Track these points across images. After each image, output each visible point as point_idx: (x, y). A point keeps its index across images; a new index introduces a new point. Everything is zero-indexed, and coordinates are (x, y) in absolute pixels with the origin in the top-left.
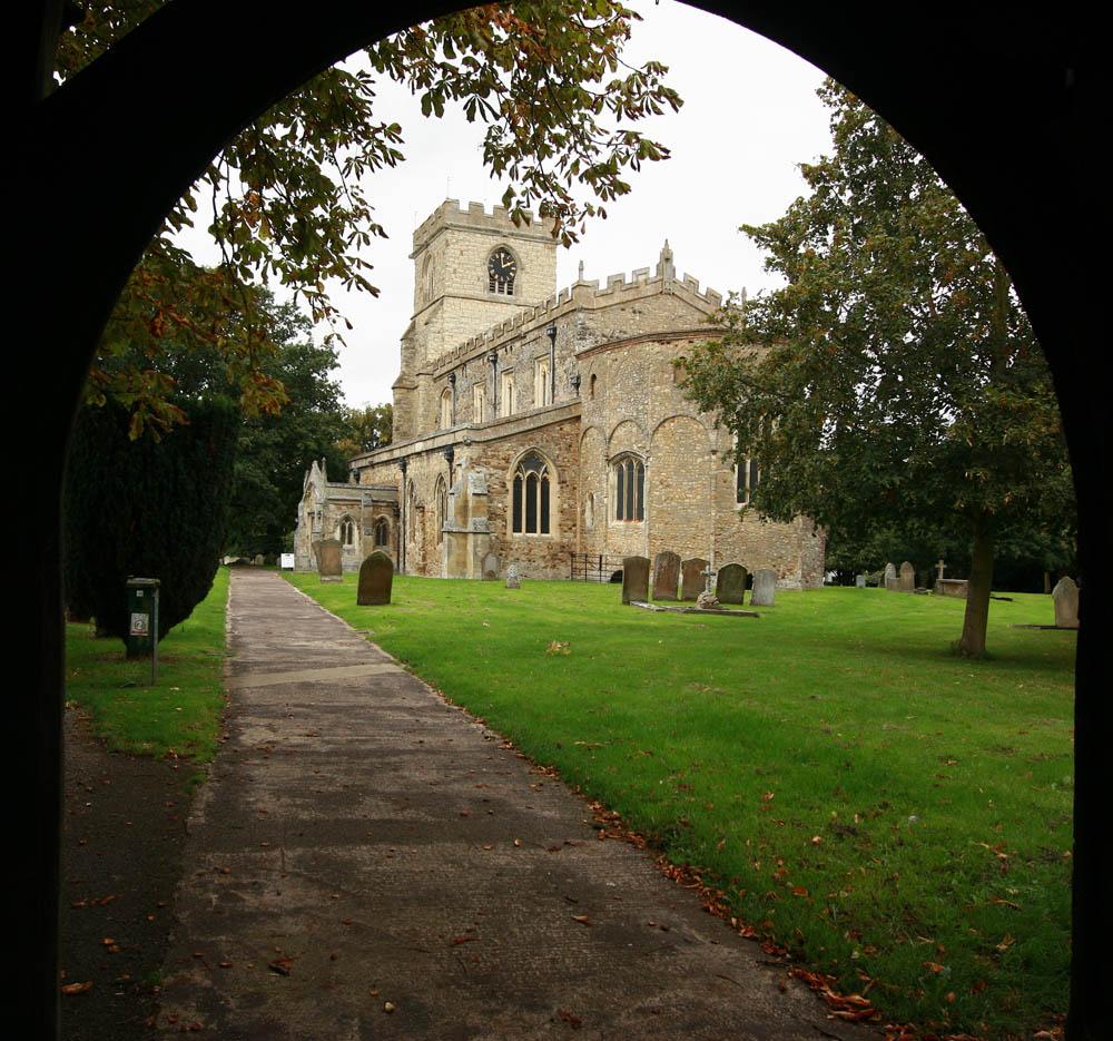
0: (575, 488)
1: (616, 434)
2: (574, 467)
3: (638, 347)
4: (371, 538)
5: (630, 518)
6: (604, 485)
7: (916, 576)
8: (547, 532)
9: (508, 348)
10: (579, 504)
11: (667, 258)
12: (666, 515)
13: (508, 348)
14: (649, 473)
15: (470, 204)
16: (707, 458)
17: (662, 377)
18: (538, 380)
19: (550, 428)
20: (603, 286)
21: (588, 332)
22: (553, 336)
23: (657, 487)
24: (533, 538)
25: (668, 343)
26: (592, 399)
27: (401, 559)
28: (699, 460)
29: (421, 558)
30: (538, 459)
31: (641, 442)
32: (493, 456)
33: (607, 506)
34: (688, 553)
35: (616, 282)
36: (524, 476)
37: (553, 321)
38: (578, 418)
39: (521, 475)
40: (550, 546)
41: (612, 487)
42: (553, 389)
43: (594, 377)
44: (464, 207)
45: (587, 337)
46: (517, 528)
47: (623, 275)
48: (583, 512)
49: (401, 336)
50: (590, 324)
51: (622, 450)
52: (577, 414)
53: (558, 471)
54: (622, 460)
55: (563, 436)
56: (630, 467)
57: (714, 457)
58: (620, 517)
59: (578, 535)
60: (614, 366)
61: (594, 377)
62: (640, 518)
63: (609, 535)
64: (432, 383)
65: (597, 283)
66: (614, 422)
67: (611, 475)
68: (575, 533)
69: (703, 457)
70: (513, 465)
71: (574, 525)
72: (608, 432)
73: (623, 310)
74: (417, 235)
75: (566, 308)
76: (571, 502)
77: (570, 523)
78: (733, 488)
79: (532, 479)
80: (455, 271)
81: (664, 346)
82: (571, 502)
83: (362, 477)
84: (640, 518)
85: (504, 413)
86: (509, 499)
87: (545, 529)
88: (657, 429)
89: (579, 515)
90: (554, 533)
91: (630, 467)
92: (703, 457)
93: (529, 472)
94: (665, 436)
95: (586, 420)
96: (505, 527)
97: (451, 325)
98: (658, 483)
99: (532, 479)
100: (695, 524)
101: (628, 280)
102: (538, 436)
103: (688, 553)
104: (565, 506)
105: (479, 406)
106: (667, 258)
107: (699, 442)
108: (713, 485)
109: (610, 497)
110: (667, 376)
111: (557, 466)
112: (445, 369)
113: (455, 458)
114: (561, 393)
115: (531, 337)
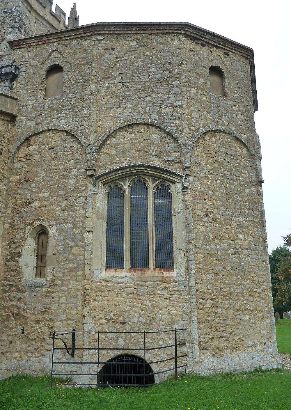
1: (113, 140)
12: (215, 261)
14: (189, 198)
25: (203, 45)
26: (45, 96)
28: (247, 191)
34: (246, 318)
41: (98, 217)
43: (55, 69)
51: (126, 163)
52: (14, 112)
54: (123, 178)
60: (107, 55)
63: (93, 294)
72: (93, 138)
81: (198, 47)
94: (206, 151)
98: (202, 214)
100: (250, 276)
103: (246, 318)
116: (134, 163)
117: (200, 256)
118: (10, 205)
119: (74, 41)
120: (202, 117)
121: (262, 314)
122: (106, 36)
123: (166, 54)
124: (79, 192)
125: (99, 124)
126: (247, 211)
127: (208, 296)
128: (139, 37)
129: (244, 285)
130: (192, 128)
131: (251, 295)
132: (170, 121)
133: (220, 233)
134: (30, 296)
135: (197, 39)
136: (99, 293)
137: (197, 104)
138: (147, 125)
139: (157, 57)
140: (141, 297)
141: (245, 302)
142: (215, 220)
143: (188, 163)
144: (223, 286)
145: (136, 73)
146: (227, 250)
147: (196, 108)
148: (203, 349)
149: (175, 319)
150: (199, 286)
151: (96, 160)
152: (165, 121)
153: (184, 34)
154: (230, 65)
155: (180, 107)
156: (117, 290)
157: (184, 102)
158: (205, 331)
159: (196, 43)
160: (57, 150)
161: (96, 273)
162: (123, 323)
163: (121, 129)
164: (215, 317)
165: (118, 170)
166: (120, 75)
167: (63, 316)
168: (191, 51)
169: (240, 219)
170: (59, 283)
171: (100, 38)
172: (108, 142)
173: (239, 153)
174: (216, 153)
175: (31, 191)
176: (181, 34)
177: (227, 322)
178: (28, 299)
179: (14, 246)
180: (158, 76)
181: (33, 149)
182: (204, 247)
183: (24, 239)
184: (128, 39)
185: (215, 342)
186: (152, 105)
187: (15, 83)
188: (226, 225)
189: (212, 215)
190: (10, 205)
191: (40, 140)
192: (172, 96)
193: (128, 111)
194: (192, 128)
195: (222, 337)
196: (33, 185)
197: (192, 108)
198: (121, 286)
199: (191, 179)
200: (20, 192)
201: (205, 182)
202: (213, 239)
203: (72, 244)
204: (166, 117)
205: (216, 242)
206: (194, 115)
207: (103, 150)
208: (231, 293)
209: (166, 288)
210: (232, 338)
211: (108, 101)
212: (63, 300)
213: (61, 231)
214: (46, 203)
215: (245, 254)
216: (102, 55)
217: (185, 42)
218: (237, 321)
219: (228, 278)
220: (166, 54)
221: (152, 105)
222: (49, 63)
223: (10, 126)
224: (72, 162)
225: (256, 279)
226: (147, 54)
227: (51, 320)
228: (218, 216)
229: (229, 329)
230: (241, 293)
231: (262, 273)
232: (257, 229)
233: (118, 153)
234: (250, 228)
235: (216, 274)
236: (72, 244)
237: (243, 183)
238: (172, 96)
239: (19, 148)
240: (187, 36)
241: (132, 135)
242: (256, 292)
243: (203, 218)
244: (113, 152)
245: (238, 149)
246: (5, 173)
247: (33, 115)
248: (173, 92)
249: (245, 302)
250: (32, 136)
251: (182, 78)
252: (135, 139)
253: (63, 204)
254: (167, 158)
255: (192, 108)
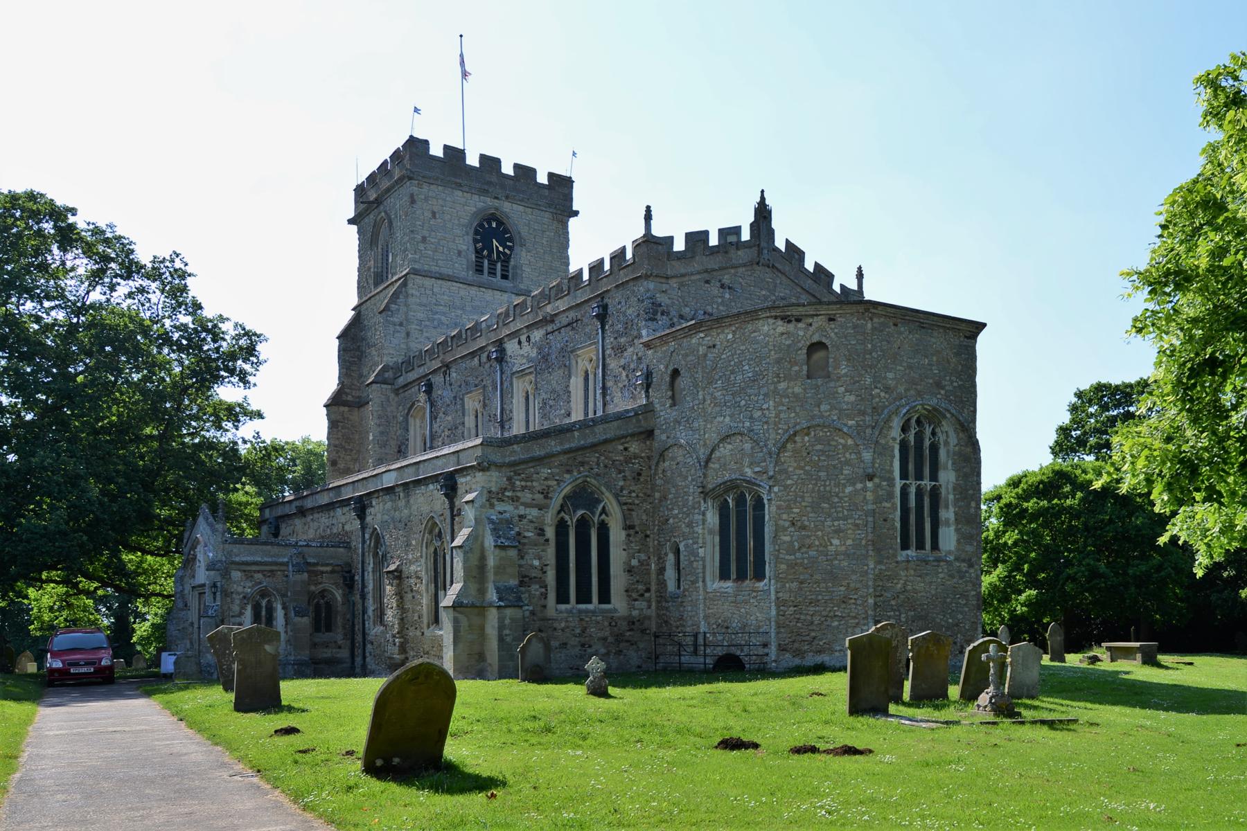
0: (647, 536)
1: (717, 454)
2: (647, 506)
3: (750, 327)
4: (305, 621)
5: (741, 576)
6: (699, 530)
7: (1111, 656)
8: (609, 602)
9: (523, 338)
10: (653, 560)
11: (763, 213)
13: (523, 338)
14: (773, 509)
15: (446, 147)
16: (859, 486)
17: (790, 369)
18: (576, 383)
19: (610, 447)
20: (679, 245)
21: (660, 309)
22: (602, 317)
23: (785, 529)
24: (587, 611)
25: (798, 320)
27: (358, 652)
28: (849, 489)
29: (396, 650)
30: (592, 493)
31: (758, 464)
32: (523, 488)
33: (703, 559)
34: (836, 623)
35: (697, 239)
36: (572, 521)
37: (602, 296)
38: (650, 434)
39: (567, 518)
40: (613, 622)
42: (604, 394)
43: (676, 373)
44: (436, 151)
45: (659, 316)
46: (562, 598)
47: (706, 233)
48: (662, 570)
49: (338, 333)
50: (660, 298)
53: (623, 511)
54: (727, 491)
55: (628, 460)
56: (741, 501)
57: (869, 484)
58: (724, 575)
59: (654, 604)
60: (709, 355)
61: (676, 373)
62: (759, 576)
64: (392, 396)
65: (670, 240)
66: (712, 437)
67: (709, 515)
68: (649, 601)
69: (854, 484)
70: (556, 501)
71: (648, 590)
72: (703, 453)
73: (707, 282)
74: (360, 191)
75: (623, 277)
76: (643, 557)
77: (641, 587)
78: (894, 528)
79: (583, 525)
80: (424, 239)
81: (791, 327)
82: (643, 557)
83: (285, 530)
84: (759, 576)
85: (517, 428)
86: (550, 553)
87: (605, 597)
88: (784, 446)
89: (653, 576)
90: (618, 602)
91: (741, 501)
92: (854, 484)
93: (580, 512)
95: (664, 437)
96: (545, 596)
97: (420, 315)
98: (787, 524)
99: (583, 525)
101: (714, 241)
102: (592, 458)
103: (836, 623)
104: (634, 562)
105: (473, 425)
106: (763, 213)
107: (848, 463)
108: (871, 525)
109: (709, 546)
110: (796, 368)
111: (621, 504)
112: (412, 376)
113: (460, 492)
114: (616, 400)
115: (564, 320)
116: (733, 477)
117: (783, 567)
118: (656, 523)
119: (685, 340)
120: (793, 415)
121: (857, 621)
122: (707, 332)
123: (756, 346)
124: (695, 509)
125: (706, 436)
126: (846, 513)
127: (791, 604)
128: (734, 329)
129: (834, 591)
130: (780, 431)
131: (844, 602)
132: (759, 427)
133: (807, 541)
134: (672, 606)
135: (789, 316)
136: (711, 602)
137: (787, 400)
138: (741, 434)
139: (749, 351)
140: (739, 605)
141: (835, 609)
142: (803, 528)
143: (771, 473)
144: (808, 593)
145: (732, 373)
146: (817, 558)
147: (784, 405)
148: (782, 650)
149: (761, 624)
150: (780, 595)
151: (705, 475)
152: (755, 428)
153: (771, 317)
154: (836, 334)
155: (768, 409)
156: (723, 599)
157: (771, 403)
158: (785, 635)
159: (789, 322)
160: (680, 466)
161: (709, 583)
162: (727, 628)
163: (723, 440)
164: (797, 622)
165: (721, 485)
166: (721, 377)
167: (690, 623)
168: (783, 334)
169: (836, 523)
170: (687, 593)
171: (702, 335)
172: (713, 456)
173: (841, 447)
174: (808, 454)
175: (667, 509)
176: (768, 317)
177: (810, 628)
178: (671, 608)
179: (661, 561)
180: (750, 375)
181: (667, 464)
182: (787, 557)
183: (666, 554)
184: (726, 331)
185: (796, 645)
186: (746, 410)
187: (650, 390)
188: (816, 532)
189: (799, 524)
190: (656, 523)
191: (670, 455)
192: (761, 397)
193: (728, 419)
194: (780, 431)
195: (804, 641)
196: (669, 502)
197: (780, 408)
198: (724, 595)
199: (776, 489)
200: (661, 509)
201: (792, 490)
202: (800, 548)
203: (692, 559)
204: (756, 423)
205: (804, 550)
206: (782, 416)
207: (711, 465)
208: (819, 601)
209: (756, 597)
210: (816, 642)
211: (713, 408)
212: (689, 608)
213: (686, 546)
214: (677, 520)
215: (840, 560)
216: (706, 355)
217: (774, 326)
218: (823, 627)
219: (815, 586)
220: (756, 346)
221: (746, 410)
222: (671, 368)
223: (648, 443)
224: (690, 479)
225: (852, 585)
226: (742, 348)
227: (684, 626)
228: (807, 523)
229: (813, 634)
230: (830, 599)
231: (861, 579)
232: (859, 532)
233: (721, 467)
234: (850, 532)
235: (802, 583)
236: (692, 559)
237: (843, 482)
238: (761, 397)
239: (658, 463)
240: (776, 317)
241: (730, 446)
242: (851, 599)
243: (788, 527)
244: (717, 466)
245: (842, 441)
246: (649, 492)
247: (664, 427)
248: (762, 392)
249: (835, 609)
250: (664, 451)
251: (770, 374)
252: (732, 450)
253: (686, 521)
254: (757, 469)
255: (780, 408)
